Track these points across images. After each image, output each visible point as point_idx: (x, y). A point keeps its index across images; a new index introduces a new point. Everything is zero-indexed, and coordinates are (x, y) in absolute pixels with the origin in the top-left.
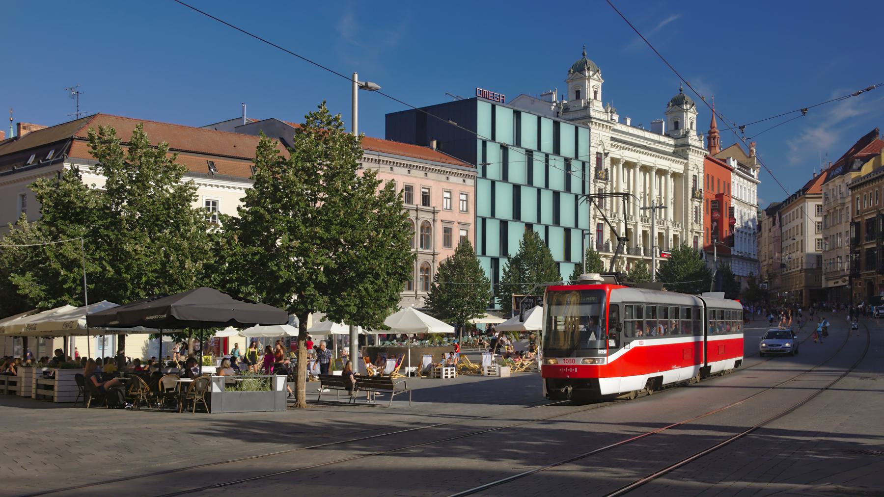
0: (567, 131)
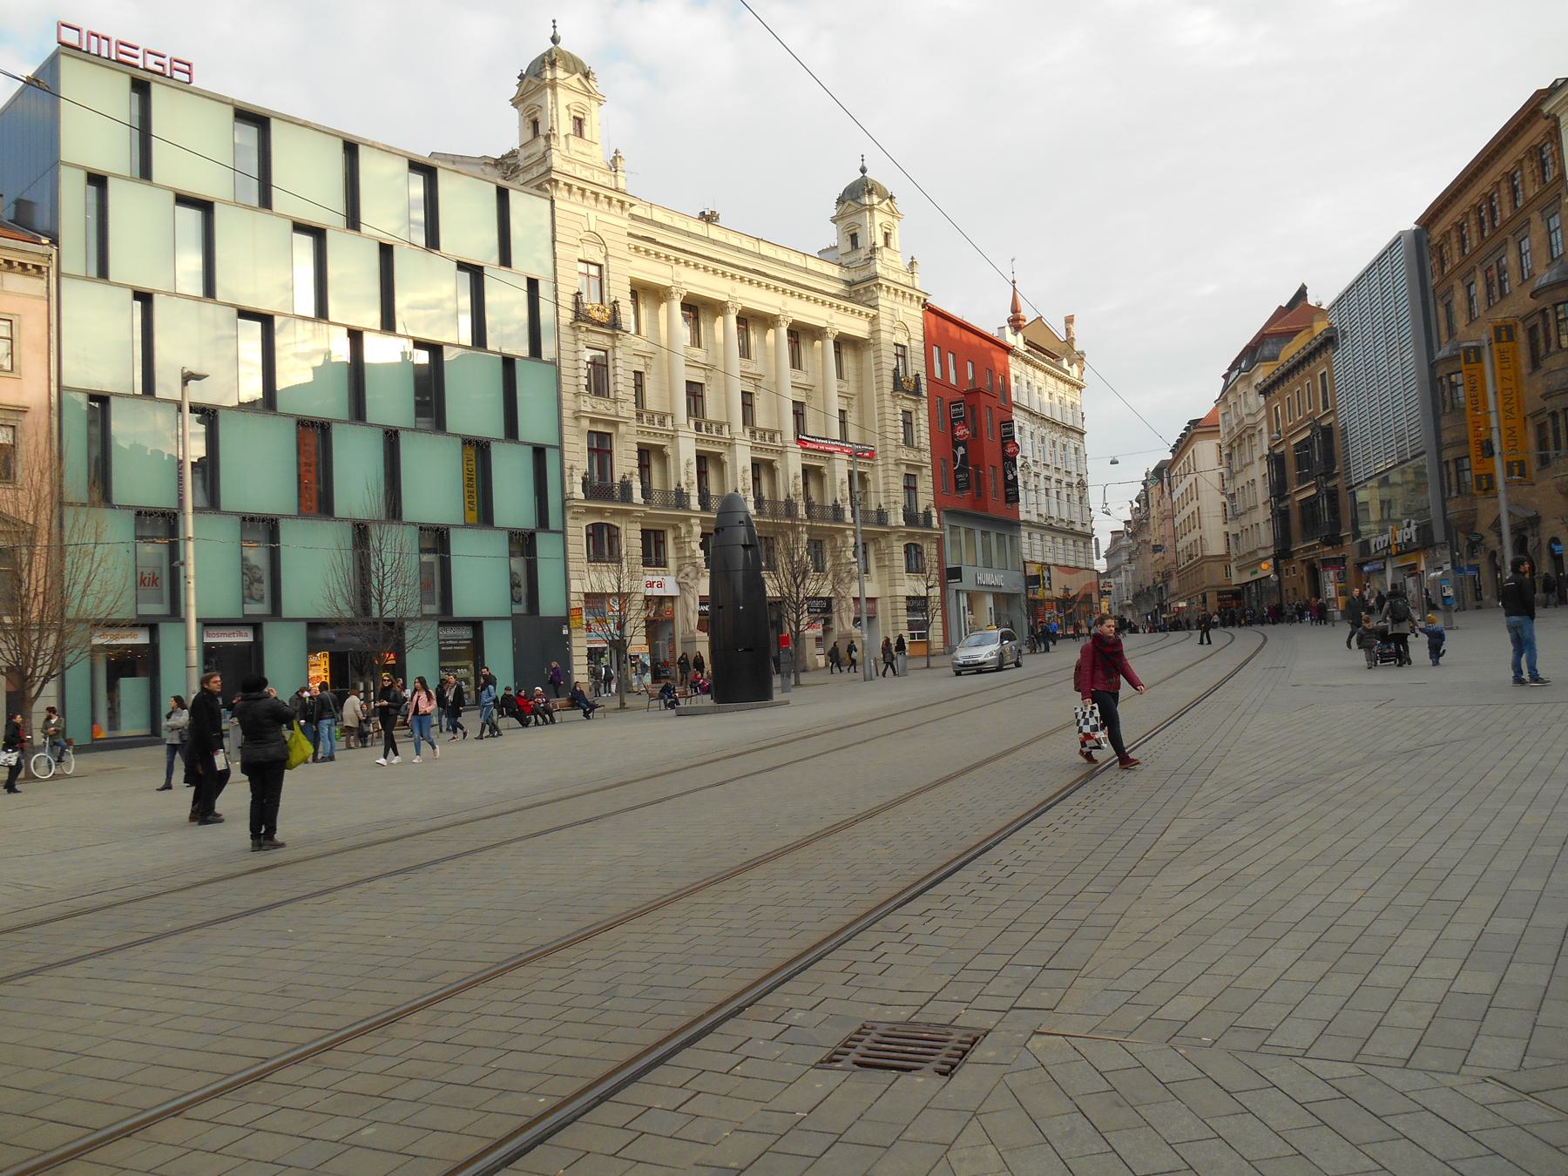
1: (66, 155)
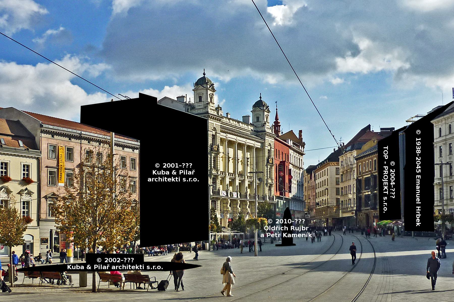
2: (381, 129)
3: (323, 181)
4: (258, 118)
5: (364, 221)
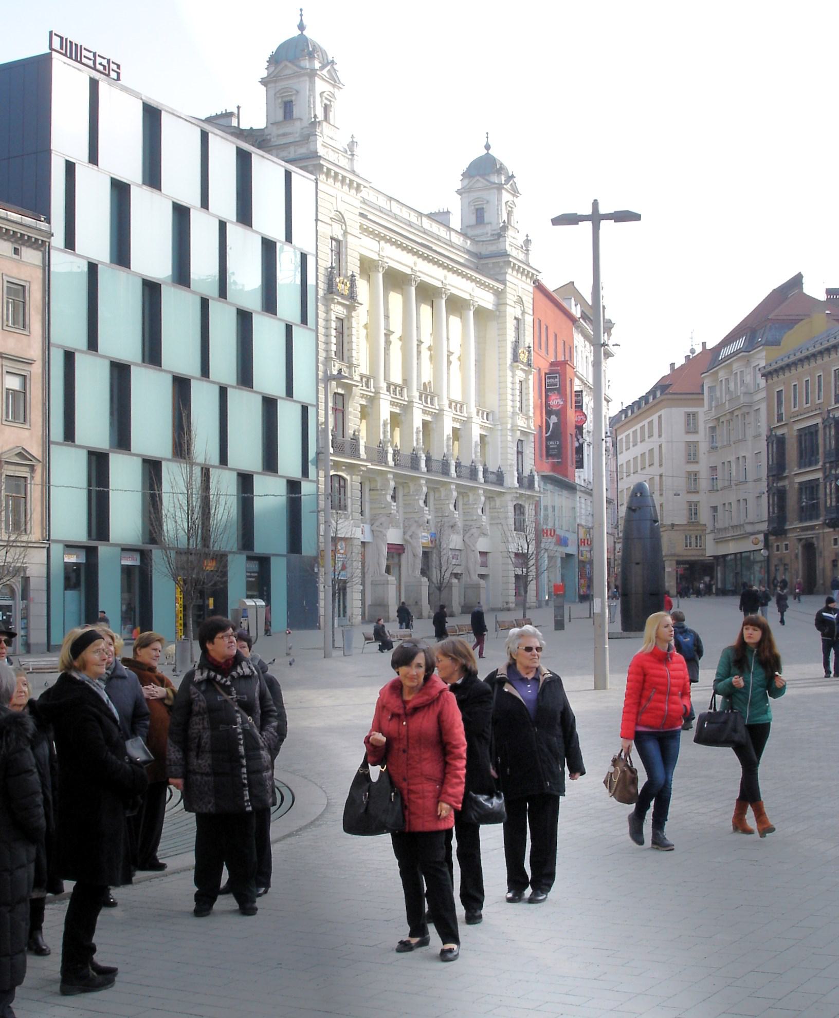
0: (267, 173)
1: (55, 144)
2: (829, 292)
3: (635, 459)
4: (480, 214)
5: (799, 566)
